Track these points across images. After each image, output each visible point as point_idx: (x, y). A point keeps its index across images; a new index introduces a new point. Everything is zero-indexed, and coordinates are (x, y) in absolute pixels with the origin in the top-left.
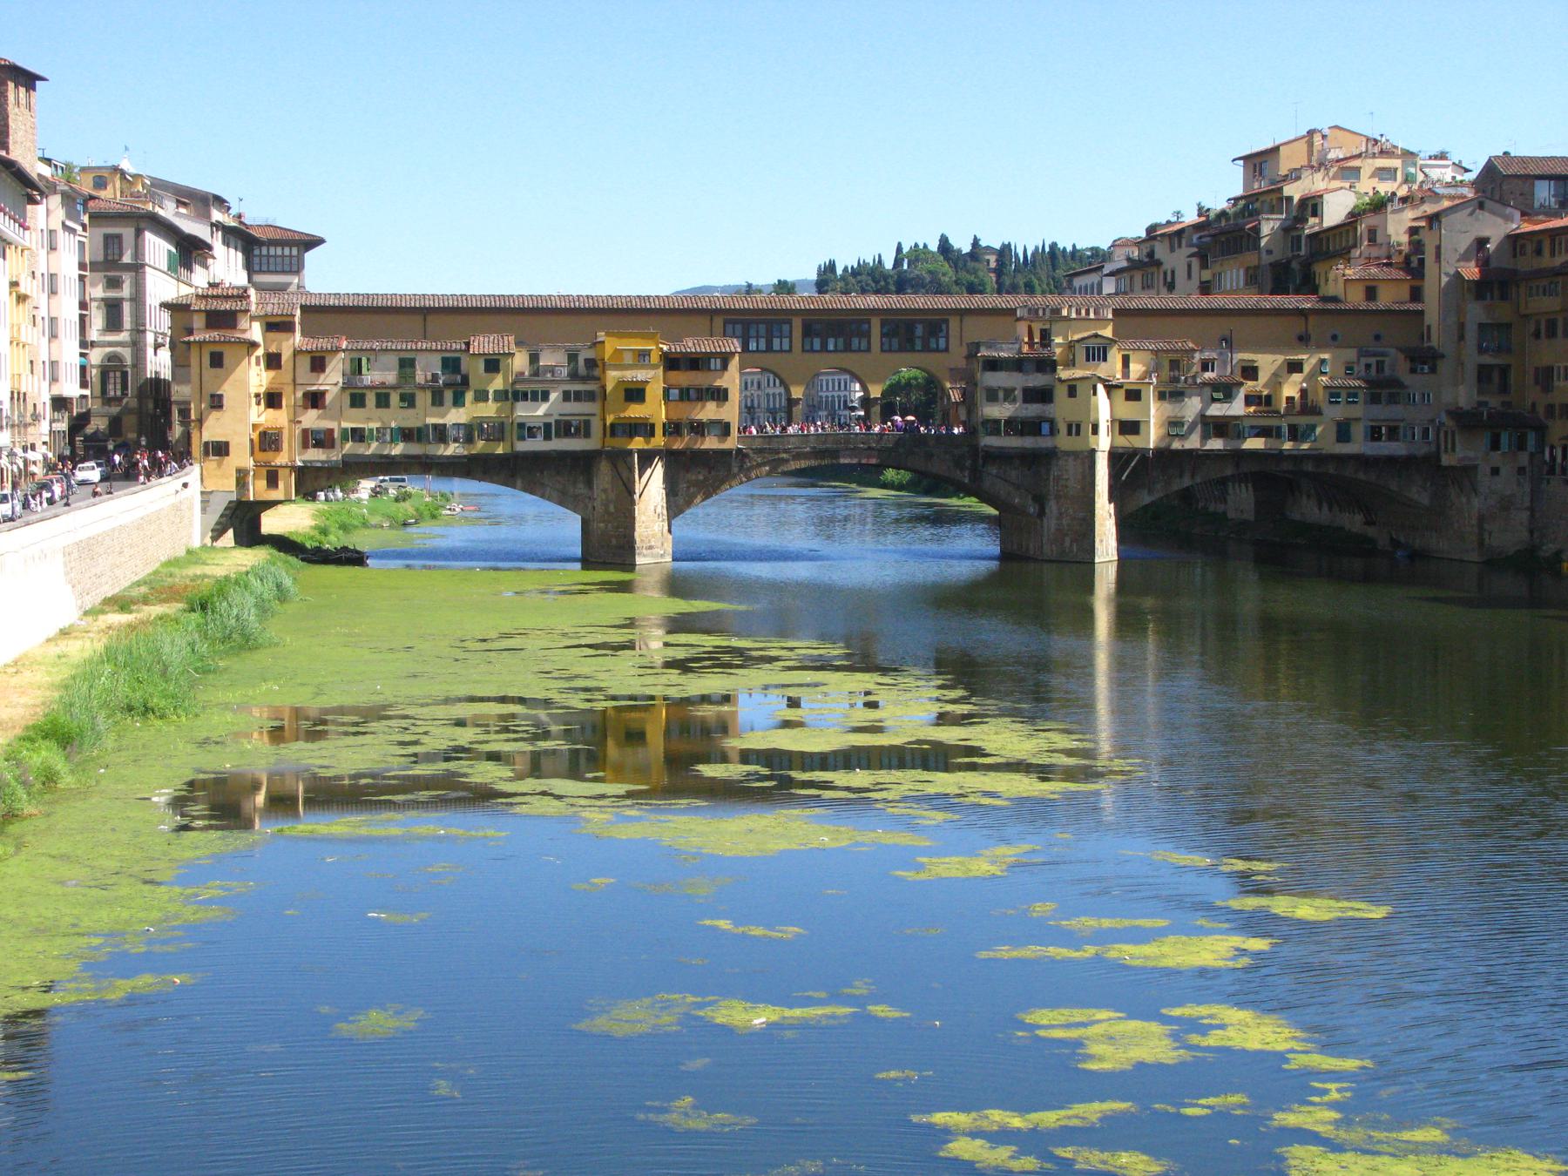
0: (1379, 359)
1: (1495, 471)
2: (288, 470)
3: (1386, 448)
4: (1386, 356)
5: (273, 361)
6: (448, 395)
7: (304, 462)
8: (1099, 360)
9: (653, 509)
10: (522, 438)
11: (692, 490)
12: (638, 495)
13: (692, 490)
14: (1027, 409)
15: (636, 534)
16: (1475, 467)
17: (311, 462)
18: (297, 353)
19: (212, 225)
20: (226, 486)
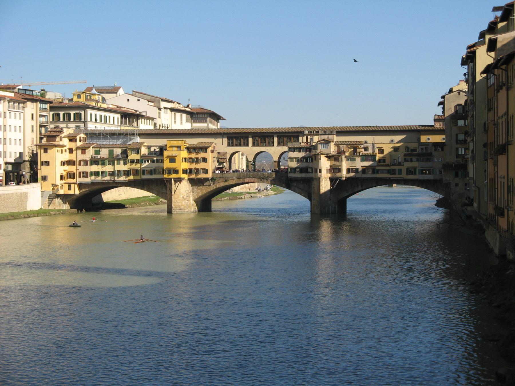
0: (426, 146)
1: (457, 185)
2: (74, 185)
3: (431, 177)
4: (428, 145)
5: (71, 151)
6: (122, 162)
7: (80, 182)
8: (325, 148)
9: (182, 197)
10: (144, 174)
11: (198, 191)
12: (174, 192)
13: (198, 191)
14: (303, 164)
15: (173, 205)
16: (450, 183)
17: (82, 182)
18: (77, 148)
19: (160, 109)
20: (49, 189)
